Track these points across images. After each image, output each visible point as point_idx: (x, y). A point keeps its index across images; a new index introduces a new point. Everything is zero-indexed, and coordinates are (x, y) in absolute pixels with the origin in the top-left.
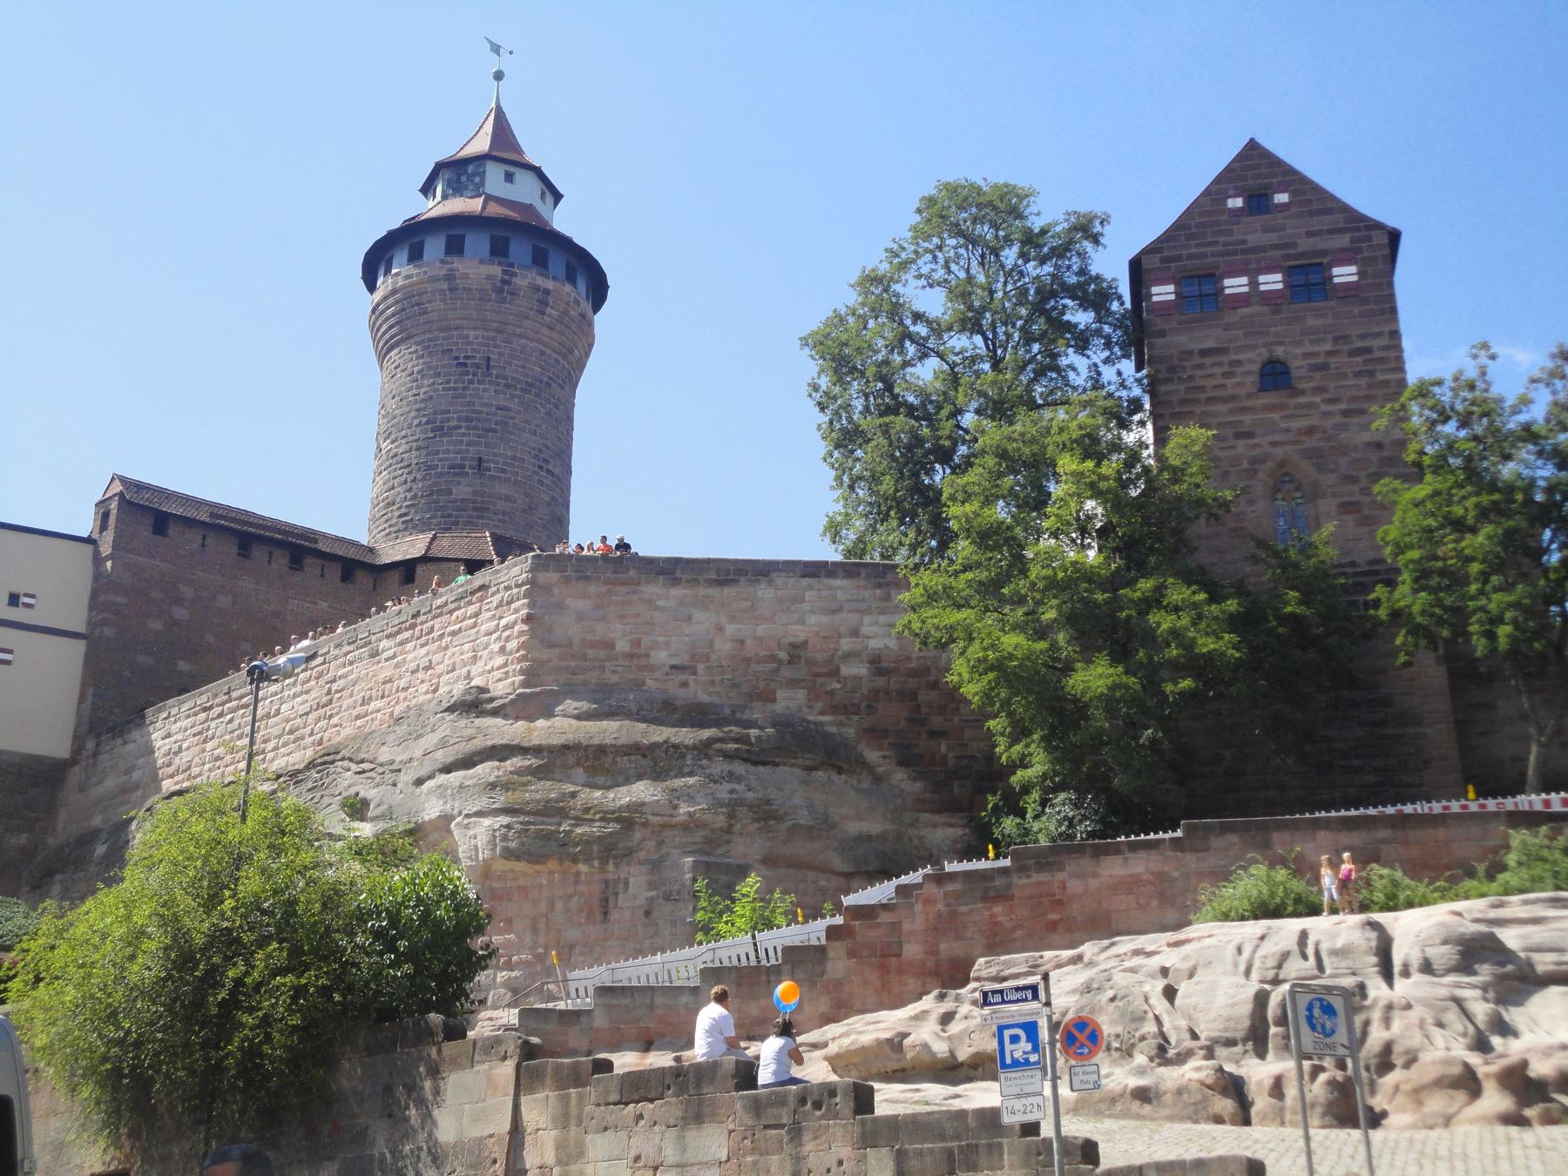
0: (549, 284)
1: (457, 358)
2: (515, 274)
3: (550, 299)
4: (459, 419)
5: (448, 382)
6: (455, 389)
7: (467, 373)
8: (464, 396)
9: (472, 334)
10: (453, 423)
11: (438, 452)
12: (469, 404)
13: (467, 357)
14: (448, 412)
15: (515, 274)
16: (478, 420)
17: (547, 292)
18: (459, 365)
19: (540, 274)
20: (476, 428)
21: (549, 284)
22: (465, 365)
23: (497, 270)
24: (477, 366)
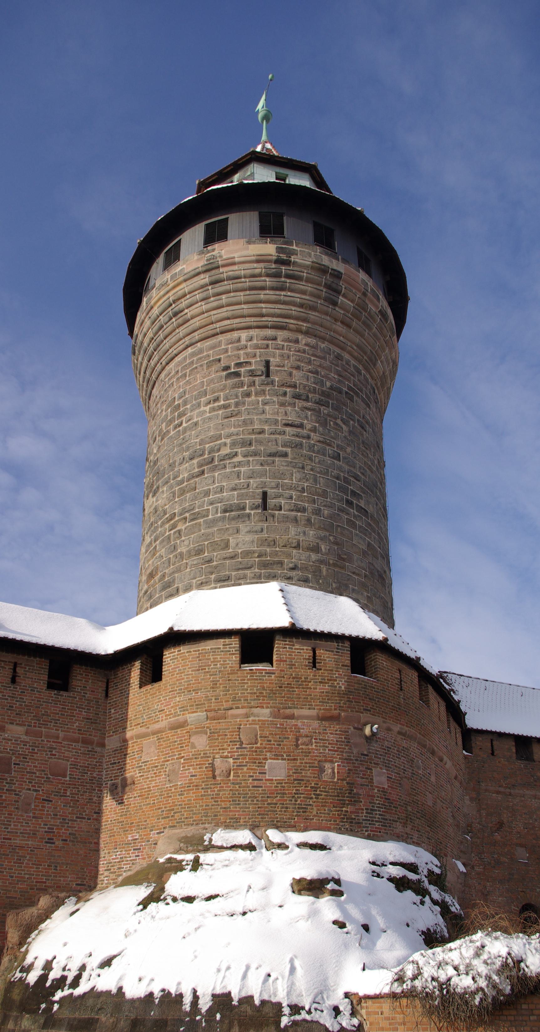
0: (340, 267)
1: (227, 368)
2: (294, 253)
3: (343, 286)
4: (233, 444)
5: (217, 399)
6: (225, 407)
7: (242, 385)
8: (238, 414)
9: (244, 335)
10: (226, 451)
11: (207, 493)
12: (245, 422)
13: (239, 365)
14: (219, 437)
15: (294, 253)
16: (260, 442)
17: (337, 275)
18: (228, 376)
19: (327, 254)
20: (255, 454)
21: (340, 267)
22: (237, 374)
23: (269, 249)
24: (252, 373)
